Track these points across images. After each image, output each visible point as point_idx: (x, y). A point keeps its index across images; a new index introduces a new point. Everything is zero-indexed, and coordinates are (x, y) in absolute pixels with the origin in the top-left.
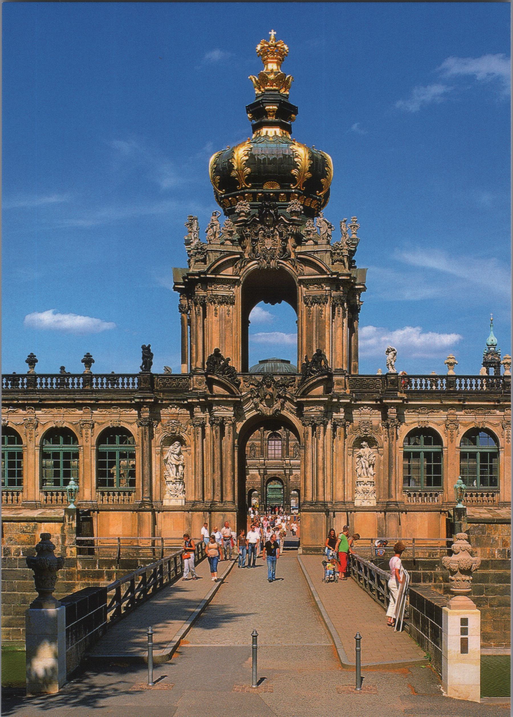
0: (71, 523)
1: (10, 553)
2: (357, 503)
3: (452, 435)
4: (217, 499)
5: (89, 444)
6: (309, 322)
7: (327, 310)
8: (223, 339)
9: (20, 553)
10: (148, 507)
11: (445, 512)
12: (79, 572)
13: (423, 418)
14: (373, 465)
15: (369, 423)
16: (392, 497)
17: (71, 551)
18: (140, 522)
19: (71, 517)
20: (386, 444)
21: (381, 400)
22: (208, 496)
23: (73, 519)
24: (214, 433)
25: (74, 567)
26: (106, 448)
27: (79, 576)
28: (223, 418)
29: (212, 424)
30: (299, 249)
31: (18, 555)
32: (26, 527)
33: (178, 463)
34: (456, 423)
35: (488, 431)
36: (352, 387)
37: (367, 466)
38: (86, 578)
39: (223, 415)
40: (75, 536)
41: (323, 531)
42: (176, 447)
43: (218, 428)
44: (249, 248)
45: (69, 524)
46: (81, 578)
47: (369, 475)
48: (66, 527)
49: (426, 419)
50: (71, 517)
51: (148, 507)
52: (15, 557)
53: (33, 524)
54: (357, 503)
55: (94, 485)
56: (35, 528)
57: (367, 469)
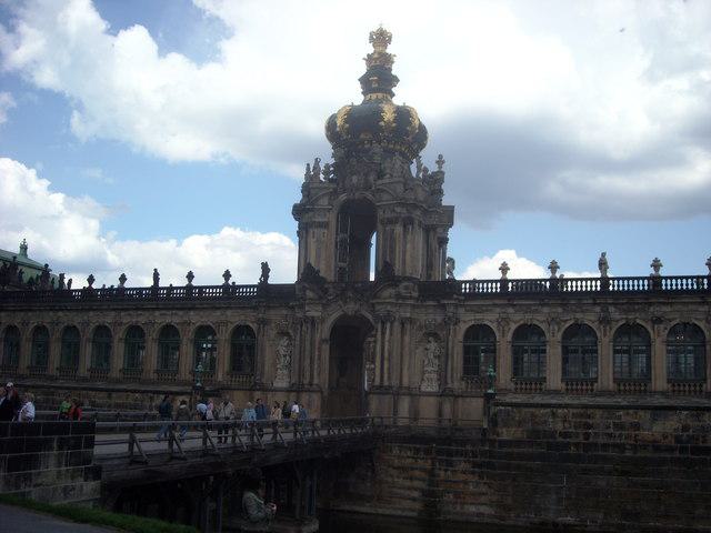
2: (423, 389)
4: (306, 381)
6: (385, 240)
7: (399, 229)
8: (318, 256)
13: (479, 316)
30: (380, 182)
36: (420, 291)
42: (284, 341)
44: (341, 184)
54: (423, 389)
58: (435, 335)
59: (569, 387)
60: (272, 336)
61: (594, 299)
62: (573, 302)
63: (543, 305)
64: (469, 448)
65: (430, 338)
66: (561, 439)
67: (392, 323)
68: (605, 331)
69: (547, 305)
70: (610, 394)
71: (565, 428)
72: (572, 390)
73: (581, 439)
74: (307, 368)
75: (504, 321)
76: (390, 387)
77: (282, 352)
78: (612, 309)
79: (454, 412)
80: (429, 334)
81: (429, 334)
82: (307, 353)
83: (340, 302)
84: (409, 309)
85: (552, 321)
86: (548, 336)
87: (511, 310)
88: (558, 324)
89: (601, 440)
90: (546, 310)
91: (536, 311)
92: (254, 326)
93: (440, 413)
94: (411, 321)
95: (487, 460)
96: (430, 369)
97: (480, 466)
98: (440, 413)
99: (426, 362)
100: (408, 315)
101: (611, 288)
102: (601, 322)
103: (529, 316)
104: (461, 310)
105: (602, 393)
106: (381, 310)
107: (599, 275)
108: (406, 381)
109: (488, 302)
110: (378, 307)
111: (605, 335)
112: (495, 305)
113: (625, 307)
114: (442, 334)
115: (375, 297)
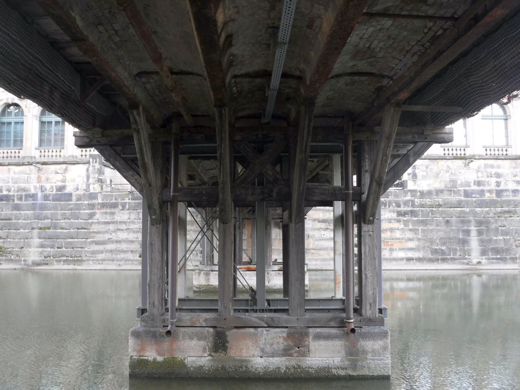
0: (94, 165)
1: (46, 189)
9: (53, 190)
12: (99, 204)
17: (94, 187)
19: (94, 160)
23: (96, 162)
25: (96, 199)
27: (99, 207)
31: (52, 191)
32: (59, 169)
38: (105, 208)
40: (96, 175)
45: (93, 166)
46: (101, 208)
48: (91, 169)
50: (94, 160)
52: (50, 193)
53: (64, 166)
56: (66, 170)
71: (478, 177)
73: (493, 187)
95: (410, 209)
97: (405, 214)
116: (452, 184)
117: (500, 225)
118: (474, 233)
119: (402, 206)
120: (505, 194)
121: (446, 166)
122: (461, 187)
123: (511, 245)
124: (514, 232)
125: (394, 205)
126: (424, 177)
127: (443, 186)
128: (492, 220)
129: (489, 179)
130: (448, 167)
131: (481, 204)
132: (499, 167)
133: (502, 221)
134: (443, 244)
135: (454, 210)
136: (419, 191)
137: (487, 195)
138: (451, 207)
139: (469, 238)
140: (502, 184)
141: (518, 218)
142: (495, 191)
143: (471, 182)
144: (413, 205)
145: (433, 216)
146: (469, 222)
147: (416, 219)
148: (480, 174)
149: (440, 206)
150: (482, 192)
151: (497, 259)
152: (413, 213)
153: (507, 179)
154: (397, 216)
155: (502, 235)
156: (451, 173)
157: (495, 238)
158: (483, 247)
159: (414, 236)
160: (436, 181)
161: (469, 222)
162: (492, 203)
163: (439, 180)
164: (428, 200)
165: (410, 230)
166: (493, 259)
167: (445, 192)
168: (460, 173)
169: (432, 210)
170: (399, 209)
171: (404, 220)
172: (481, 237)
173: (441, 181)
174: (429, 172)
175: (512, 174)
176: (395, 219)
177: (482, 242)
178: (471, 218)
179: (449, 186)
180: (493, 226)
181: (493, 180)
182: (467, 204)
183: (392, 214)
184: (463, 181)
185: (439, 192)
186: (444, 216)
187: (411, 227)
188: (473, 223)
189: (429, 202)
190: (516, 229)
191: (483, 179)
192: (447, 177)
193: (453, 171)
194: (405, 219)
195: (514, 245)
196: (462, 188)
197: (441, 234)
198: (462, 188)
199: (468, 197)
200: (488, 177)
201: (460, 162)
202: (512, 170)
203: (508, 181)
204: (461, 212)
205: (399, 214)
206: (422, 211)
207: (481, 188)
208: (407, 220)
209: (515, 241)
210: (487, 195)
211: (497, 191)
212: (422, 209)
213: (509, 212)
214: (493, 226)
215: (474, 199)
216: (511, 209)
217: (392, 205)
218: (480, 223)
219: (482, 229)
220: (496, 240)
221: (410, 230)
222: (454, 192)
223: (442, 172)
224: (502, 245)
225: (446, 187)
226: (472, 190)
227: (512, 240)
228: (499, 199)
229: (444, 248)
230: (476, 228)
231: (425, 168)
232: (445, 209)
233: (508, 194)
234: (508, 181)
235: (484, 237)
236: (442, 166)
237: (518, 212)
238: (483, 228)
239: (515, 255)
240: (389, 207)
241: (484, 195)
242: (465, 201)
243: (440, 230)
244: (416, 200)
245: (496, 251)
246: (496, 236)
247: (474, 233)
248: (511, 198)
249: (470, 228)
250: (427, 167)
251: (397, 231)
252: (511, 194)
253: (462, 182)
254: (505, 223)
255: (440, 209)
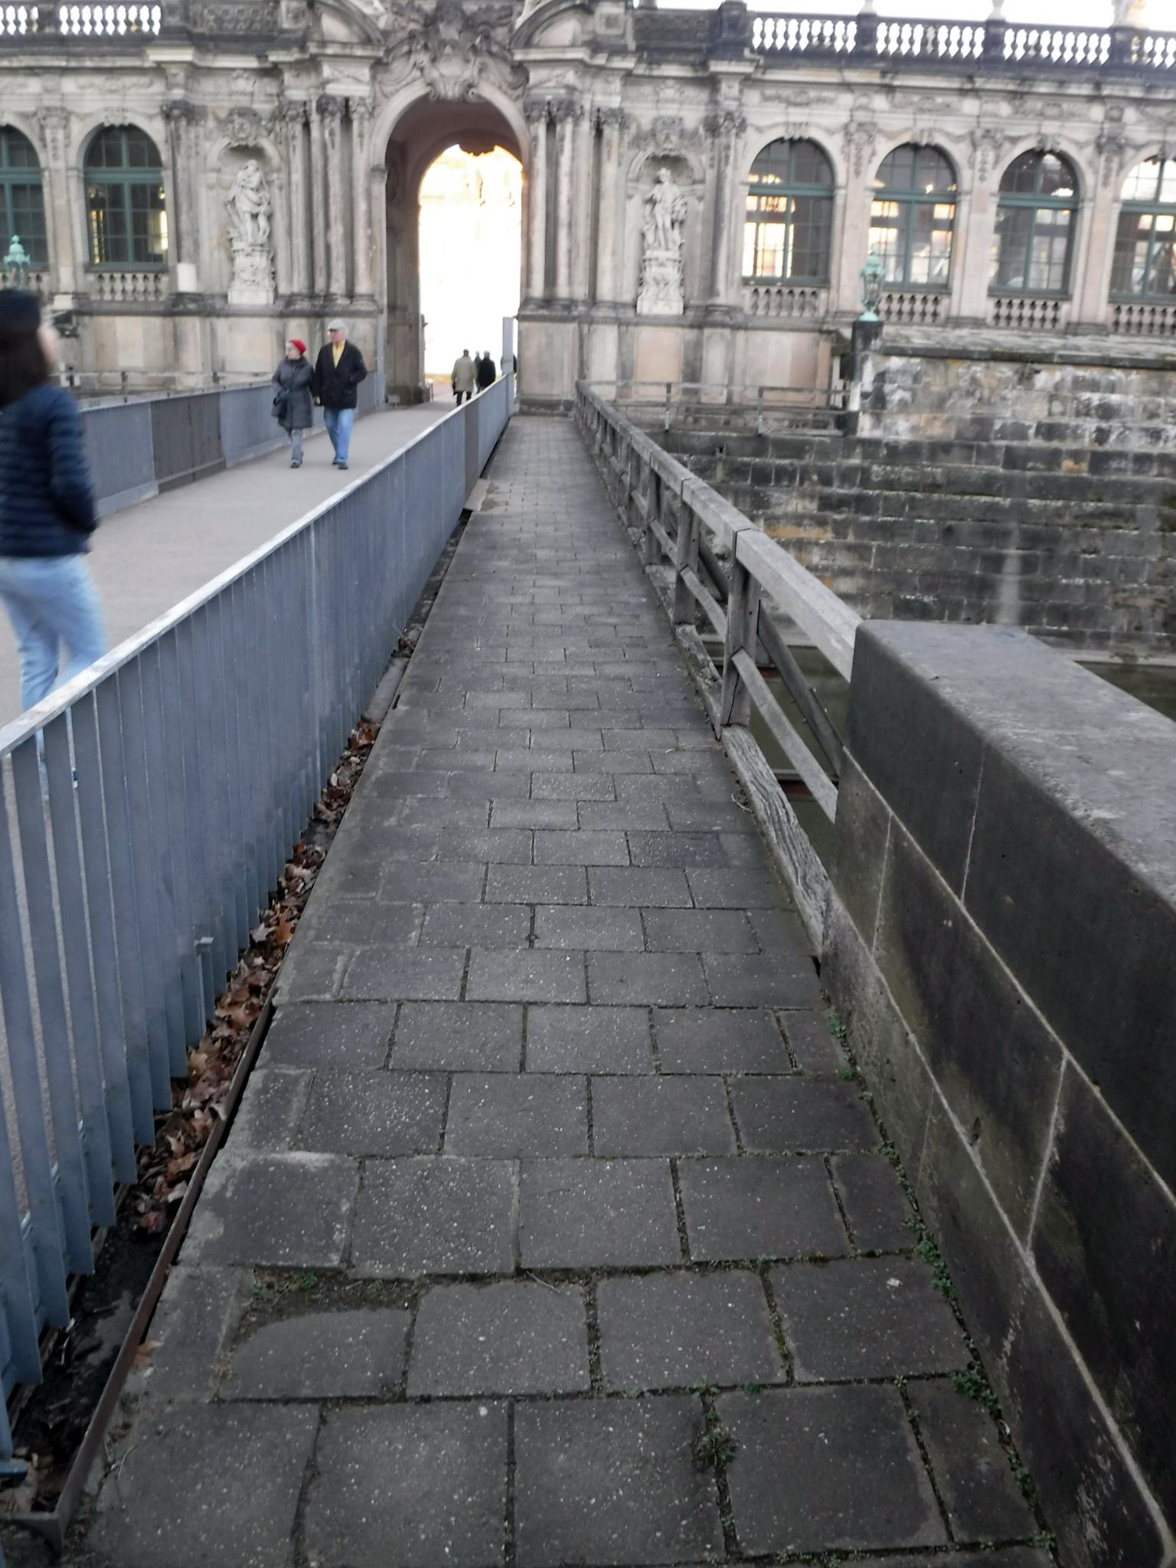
2: (645, 307)
3: (859, 157)
4: (338, 287)
5: (60, 164)
10: (192, 306)
11: (829, 332)
13: (797, 115)
14: (682, 223)
15: (675, 122)
16: (718, 295)
18: (177, 341)
20: (710, 175)
21: (704, 65)
22: (320, 283)
24: (327, 135)
26: (107, 175)
28: (347, 100)
29: (322, 110)
33: (256, 210)
34: (869, 130)
35: (940, 152)
37: (668, 224)
39: (347, 94)
41: (566, 364)
42: (250, 172)
43: (337, 124)
47: (670, 245)
49: (803, 119)
51: (192, 306)
55: (81, 256)
57: (665, 230)
58: (674, 162)
59: (1004, 311)
60: (213, 160)
61: (1098, 86)
62: (1043, 88)
63: (962, 92)
64: (809, 460)
65: (664, 173)
66: (1035, 442)
67: (576, 123)
68: (1108, 170)
69: (976, 92)
70: (1100, 329)
71: (1050, 414)
72: (1009, 318)
73: (1087, 442)
74: (338, 249)
75: (859, 131)
76: (571, 304)
77: (245, 206)
78: (1130, 114)
79: (730, 369)
80: (658, 161)
81: (658, 161)
82: (336, 208)
83: (423, 58)
84: (617, 84)
85: (983, 137)
86: (966, 176)
87: (880, 102)
88: (998, 146)
89: (1138, 444)
90: (970, 105)
91: (947, 109)
92: (156, 130)
93: (693, 371)
94: (622, 118)
95: (854, 491)
96: (662, 254)
97: (839, 504)
98: (693, 371)
99: (650, 237)
100: (615, 102)
101: (1134, 57)
102: (1099, 148)
103: (925, 122)
104: (753, 96)
105: (1074, 328)
106: (547, 83)
107: (1107, 22)
108: (606, 290)
109: (831, 76)
110: (535, 76)
111: (1105, 183)
112: (847, 86)
113: (1163, 111)
114: (699, 160)
115: (528, 44)
116: (977, 428)
117: (1084, 546)
118: (1011, 567)
119: (836, 483)
120: (1114, 465)
121: (967, 377)
122: (1002, 438)
123: (1104, 601)
124: (1117, 569)
125: (815, 478)
126: (904, 407)
127: (953, 434)
128: (1066, 534)
129: (1080, 421)
130: (974, 380)
131: (1046, 488)
132: (1112, 388)
133: (1093, 536)
134: (929, 589)
135: (972, 502)
136: (887, 445)
137: (1068, 464)
138: (964, 493)
139: (998, 576)
140: (1113, 437)
141: (1136, 532)
142: (1088, 457)
143: (1029, 427)
144: (866, 482)
145: (915, 513)
146: (1006, 534)
147: (867, 518)
148: (1057, 407)
149: (935, 487)
150: (1053, 458)
151: (1060, 634)
152: (861, 504)
153: (1129, 425)
154: (820, 509)
155: (1084, 575)
156: (980, 399)
157: (1064, 581)
158: (1029, 603)
159: (857, 563)
160: (935, 418)
161: (1006, 534)
162: (1075, 488)
163: (945, 416)
164: (907, 469)
165: (850, 548)
166: (1050, 633)
167: (956, 452)
168: (1004, 399)
169: (913, 499)
170: (828, 490)
171: (835, 521)
172: (1028, 577)
173: (948, 421)
174: (920, 394)
175: (1145, 410)
176: (812, 517)
177: (1028, 590)
178: (1012, 525)
179: (970, 434)
180: (1066, 550)
181: (1091, 425)
182: (1007, 486)
183: (807, 503)
184: (1010, 421)
185: (938, 449)
186: (942, 515)
187: (851, 539)
188: (1015, 537)
189: (908, 474)
190: (1123, 562)
191: (1064, 420)
192: (965, 409)
193: (986, 393)
194: (838, 517)
195: (1110, 600)
196: (1003, 443)
197: (927, 563)
198: (1003, 443)
199: (1014, 467)
200: (1078, 414)
201: (1006, 371)
202: (1145, 399)
203: (1130, 429)
204: (991, 507)
205: (828, 503)
206: (886, 498)
207: (1055, 444)
208: (843, 521)
209: (1115, 592)
210: (1068, 464)
211: (1094, 454)
212: (887, 493)
213: (1114, 514)
214: (1066, 550)
215: (1029, 474)
216: (1124, 506)
217: (810, 479)
218: (1031, 540)
219: (1036, 557)
220: (1067, 586)
221: (850, 548)
222: (980, 451)
223: (956, 395)
224: (1079, 600)
225: (959, 436)
226: (1029, 450)
227: (1107, 590)
228: (1096, 478)
229: (928, 599)
230: (1020, 552)
231: (909, 382)
232: (949, 497)
233: (1123, 464)
234: (1130, 429)
235: (1038, 577)
236: (958, 377)
237: (1139, 515)
238: (1039, 553)
239: (1108, 627)
240: (802, 483)
241: (1059, 465)
242: (1005, 478)
243: (924, 553)
244: (875, 468)
245: (1062, 615)
246: (1068, 577)
247: (1011, 567)
248: (1129, 477)
249: (1005, 551)
250: (916, 378)
251: (816, 550)
252: (1131, 465)
253: (1003, 426)
254: (1099, 543)
255: (936, 496)
